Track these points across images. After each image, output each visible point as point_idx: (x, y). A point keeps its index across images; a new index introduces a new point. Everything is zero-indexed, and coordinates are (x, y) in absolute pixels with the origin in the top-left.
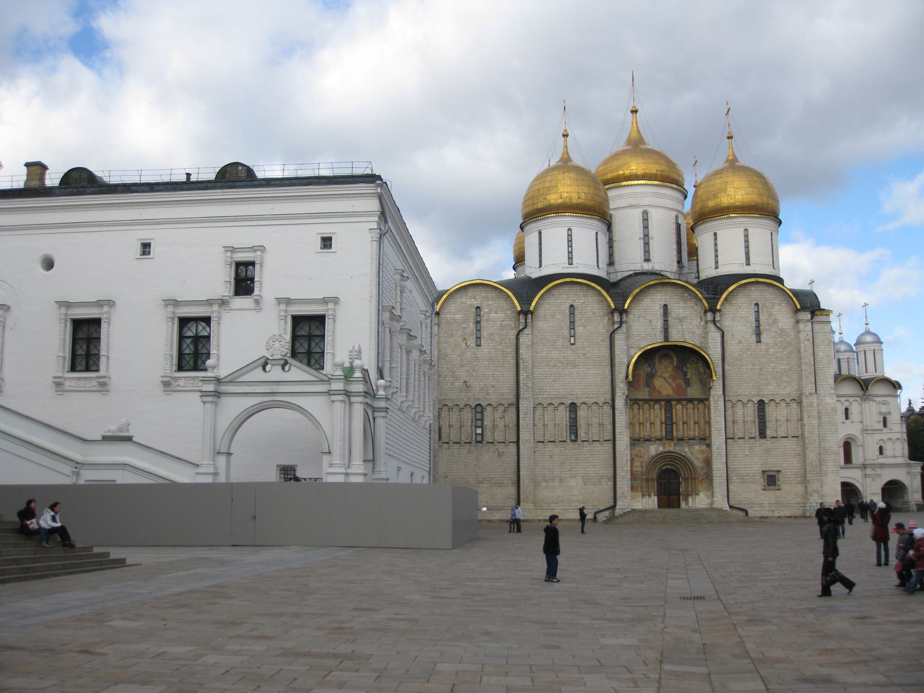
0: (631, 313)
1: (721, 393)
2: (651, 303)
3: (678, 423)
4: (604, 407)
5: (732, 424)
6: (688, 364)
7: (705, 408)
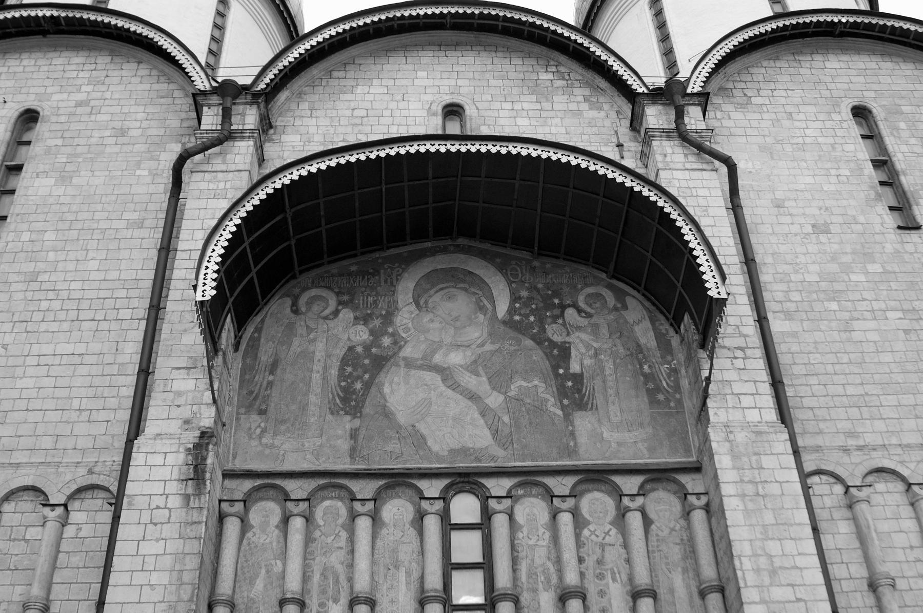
0: (289, 130)
1: (772, 415)
2: (387, 98)
3: (525, 598)
4: (75, 517)
5: (870, 600)
6: (570, 313)
7: (687, 514)
